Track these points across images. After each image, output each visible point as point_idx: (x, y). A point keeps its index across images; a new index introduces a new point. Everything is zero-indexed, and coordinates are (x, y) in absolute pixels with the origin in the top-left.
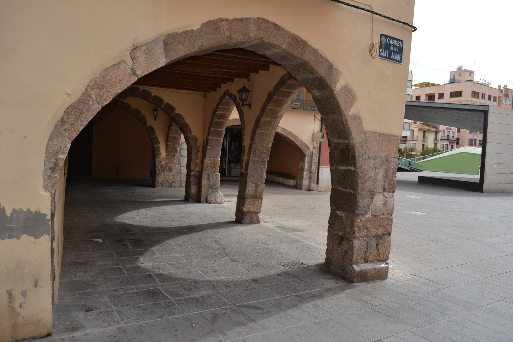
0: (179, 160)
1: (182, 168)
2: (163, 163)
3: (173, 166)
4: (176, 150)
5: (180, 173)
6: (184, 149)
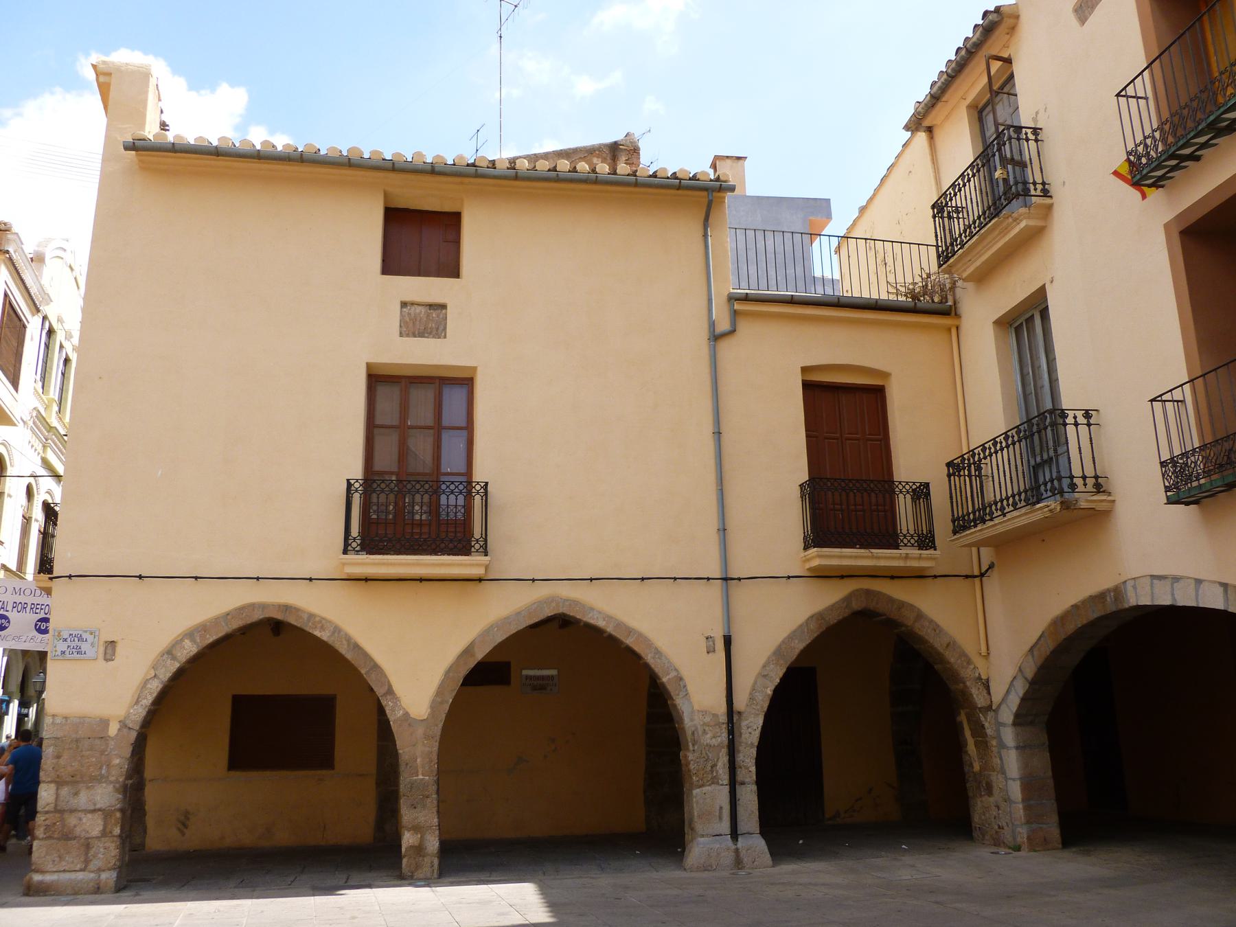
0: (1001, 759)
1: (1010, 782)
2: (977, 767)
3: (994, 778)
4: (983, 726)
5: (1007, 800)
6: (1003, 725)
